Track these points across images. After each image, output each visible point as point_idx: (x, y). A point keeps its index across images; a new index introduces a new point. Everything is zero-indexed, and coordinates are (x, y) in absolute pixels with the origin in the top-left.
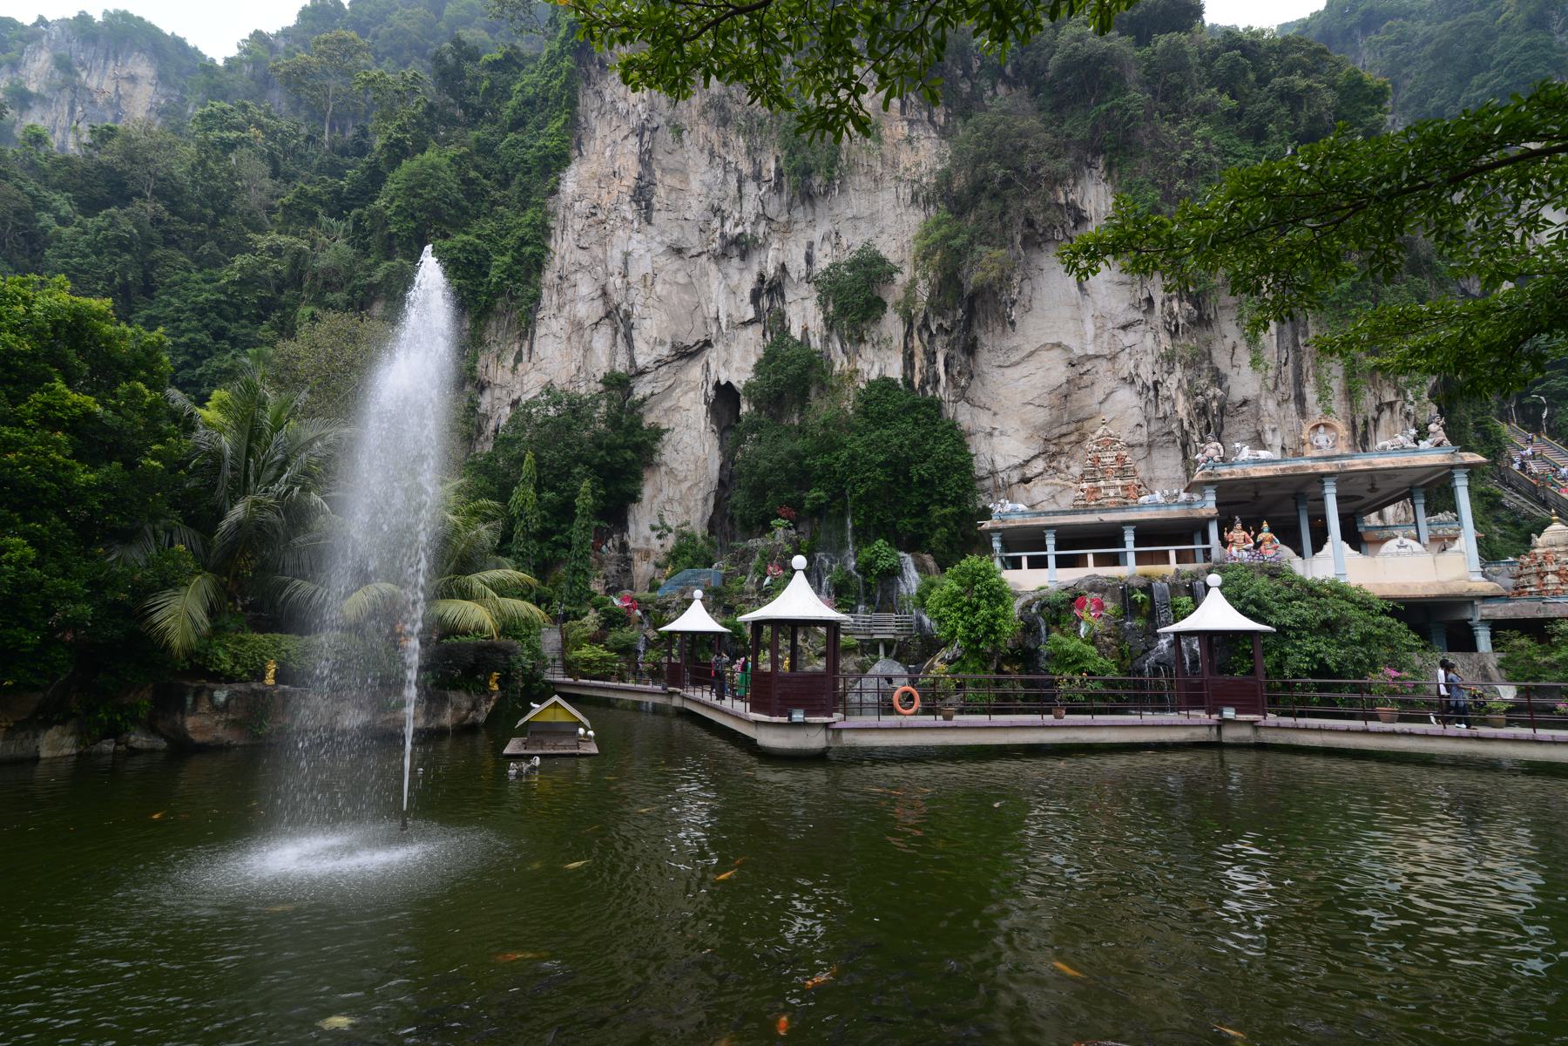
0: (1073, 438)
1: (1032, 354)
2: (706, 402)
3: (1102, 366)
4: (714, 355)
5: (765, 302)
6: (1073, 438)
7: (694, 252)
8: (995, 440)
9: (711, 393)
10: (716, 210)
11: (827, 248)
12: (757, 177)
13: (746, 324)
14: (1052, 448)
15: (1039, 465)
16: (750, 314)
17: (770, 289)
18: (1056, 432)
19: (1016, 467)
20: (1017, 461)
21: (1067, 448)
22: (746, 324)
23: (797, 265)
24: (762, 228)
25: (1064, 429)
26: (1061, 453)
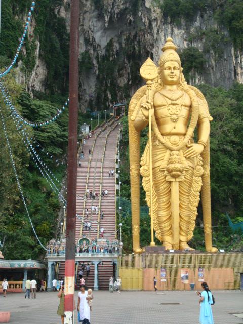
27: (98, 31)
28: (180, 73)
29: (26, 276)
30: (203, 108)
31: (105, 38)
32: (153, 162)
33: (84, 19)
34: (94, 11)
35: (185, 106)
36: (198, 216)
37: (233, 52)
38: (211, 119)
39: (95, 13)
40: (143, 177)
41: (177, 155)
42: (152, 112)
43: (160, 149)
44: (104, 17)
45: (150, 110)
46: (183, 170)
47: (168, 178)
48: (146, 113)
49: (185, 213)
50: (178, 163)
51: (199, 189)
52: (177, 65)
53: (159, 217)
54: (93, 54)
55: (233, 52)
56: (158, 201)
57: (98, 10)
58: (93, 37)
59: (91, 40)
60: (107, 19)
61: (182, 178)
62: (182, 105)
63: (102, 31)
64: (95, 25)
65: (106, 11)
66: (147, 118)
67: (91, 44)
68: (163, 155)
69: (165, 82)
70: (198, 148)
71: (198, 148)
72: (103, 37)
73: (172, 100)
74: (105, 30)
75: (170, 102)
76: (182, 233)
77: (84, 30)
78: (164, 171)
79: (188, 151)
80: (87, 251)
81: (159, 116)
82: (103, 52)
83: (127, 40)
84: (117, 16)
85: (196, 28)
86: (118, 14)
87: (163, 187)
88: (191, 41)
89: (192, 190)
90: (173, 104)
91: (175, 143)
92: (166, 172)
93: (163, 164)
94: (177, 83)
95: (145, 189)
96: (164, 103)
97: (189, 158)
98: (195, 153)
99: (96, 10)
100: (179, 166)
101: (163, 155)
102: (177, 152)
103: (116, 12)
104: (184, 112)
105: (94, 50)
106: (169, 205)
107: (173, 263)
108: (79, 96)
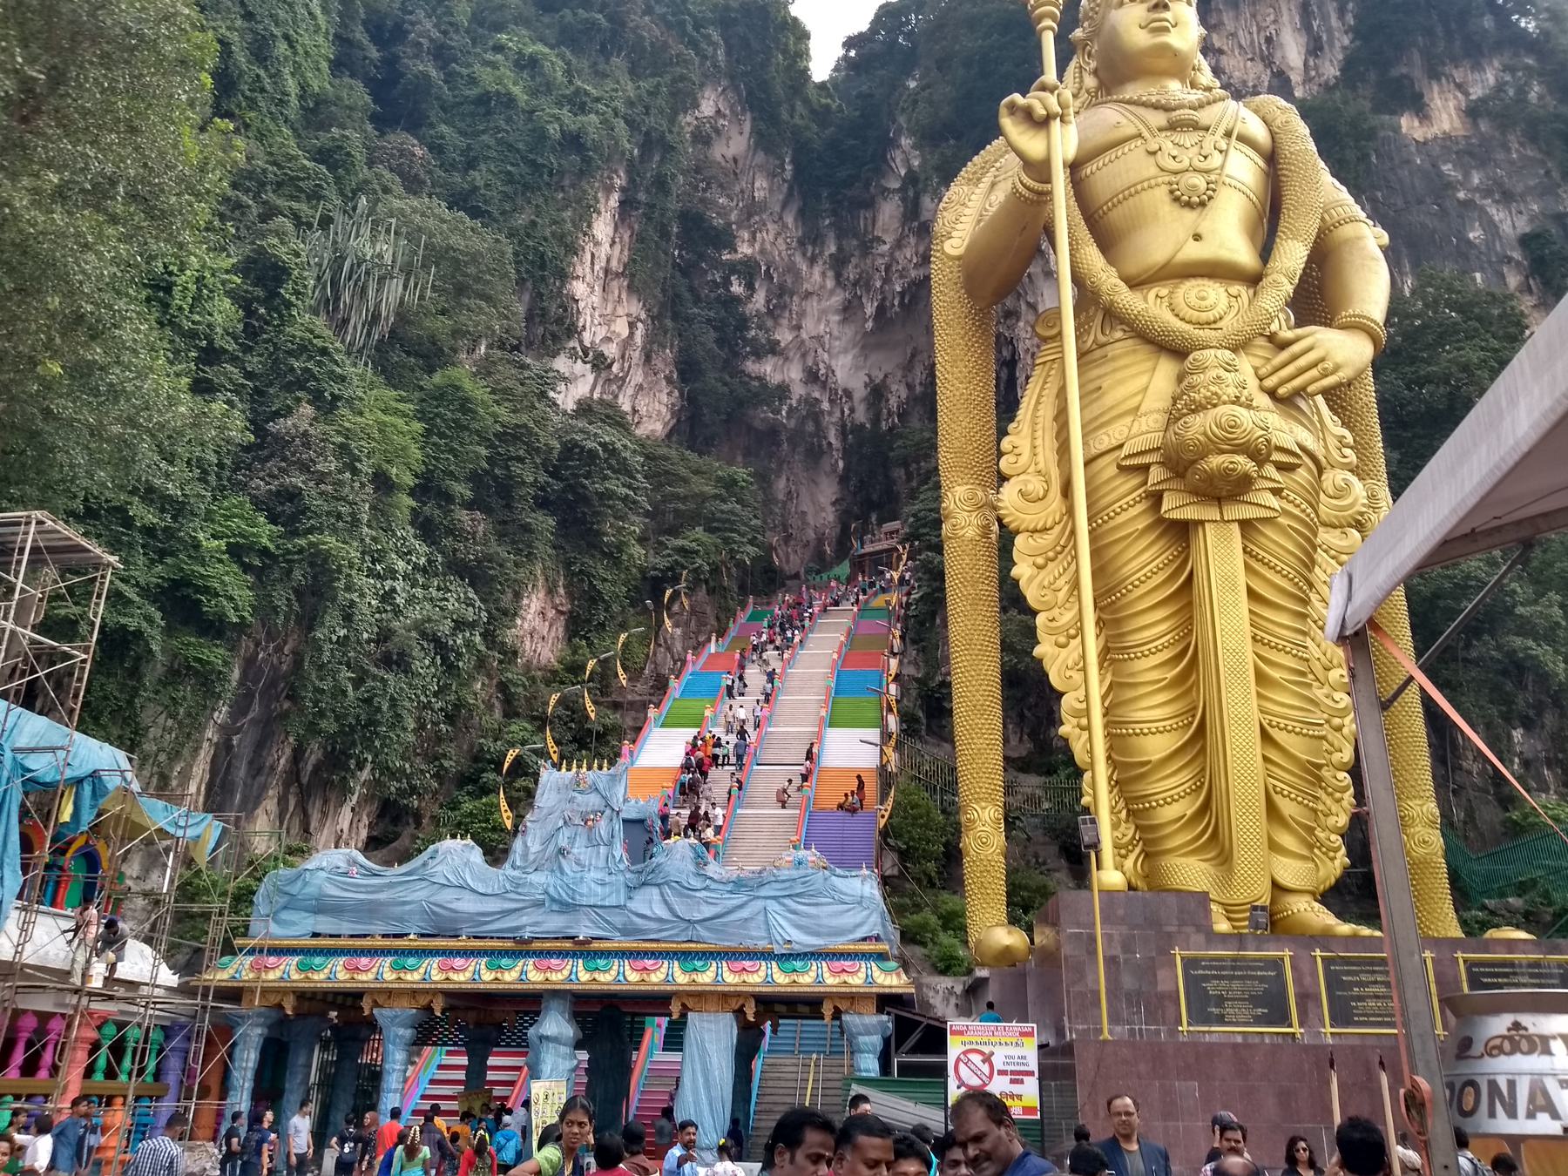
27: (845, 351)
33: (802, 314)
34: (832, 292)
35: (1242, 139)
39: (838, 299)
40: (1018, 532)
41: (1229, 367)
43: (1114, 359)
44: (862, 306)
45: (1056, 125)
46: (1267, 460)
47: (1175, 507)
48: (1033, 145)
50: (1236, 401)
54: (830, 413)
57: (844, 288)
58: (828, 367)
59: (823, 371)
60: (870, 309)
62: (1228, 134)
63: (855, 351)
64: (836, 333)
65: (868, 287)
67: (824, 385)
68: (1144, 379)
72: (857, 368)
73: (1167, 109)
74: (868, 344)
75: (1159, 119)
76: (1287, 840)
77: (803, 342)
78: (1145, 468)
79: (1284, 355)
82: (861, 416)
84: (902, 304)
86: (902, 294)
89: (1314, 597)
90: (1173, 127)
91: (1204, 316)
92: (1156, 474)
93: (1142, 431)
95: (1032, 595)
96: (1131, 130)
97: (1300, 392)
98: (1329, 365)
99: (839, 291)
101: (1144, 379)
103: (899, 289)
104: (1244, 169)
105: (831, 401)
106: (1190, 664)
107: (1284, 1019)
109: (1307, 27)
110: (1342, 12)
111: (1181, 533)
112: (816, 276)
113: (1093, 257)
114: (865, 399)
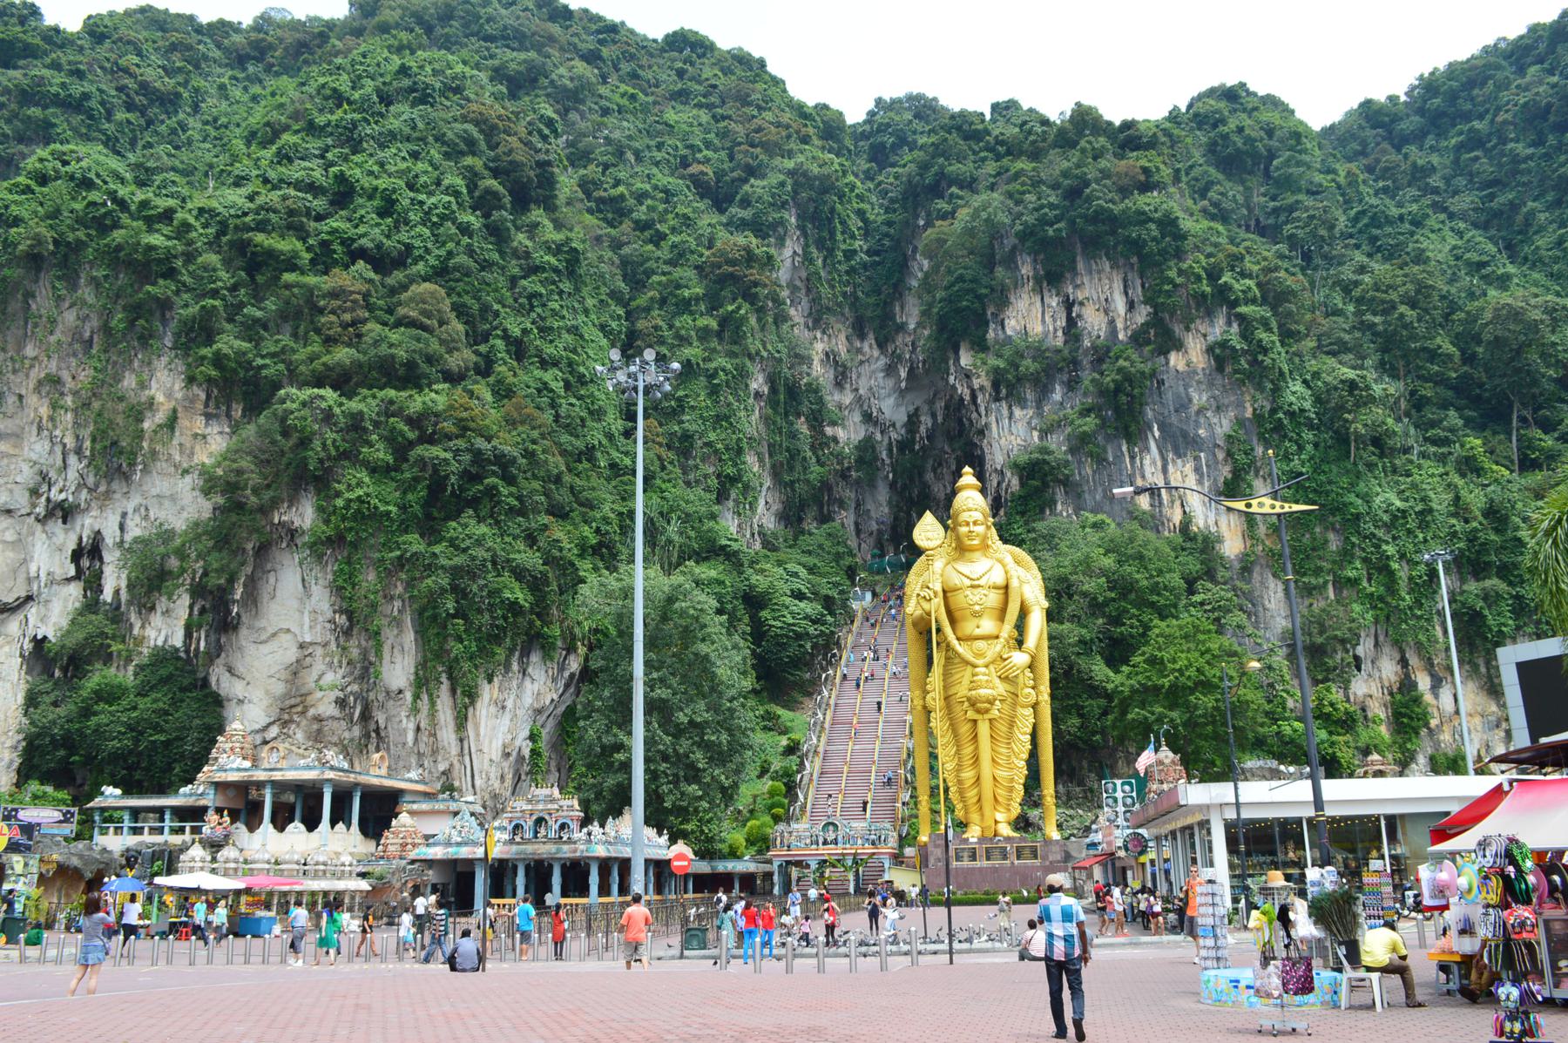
0: (299, 709)
1: (274, 635)
2: (22, 655)
3: (319, 651)
4: (34, 610)
5: (85, 563)
6: (299, 709)
7: (24, 512)
8: (245, 707)
9: (28, 646)
10: (44, 477)
11: (137, 519)
12: (78, 451)
13: (69, 580)
14: (286, 717)
15: (274, 731)
16: (72, 572)
17: (88, 555)
18: (288, 703)
19: (257, 732)
20: (257, 727)
21: (295, 717)
22: (69, 580)
23: (111, 534)
24: (84, 494)
25: (293, 701)
26: (291, 721)
28: (988, 528)
29: (737, 886)
30: (1032, 588)
31: (903, 409)
32: (946, 688)
36: (1027, 777)
37: (1124, 448)
38: (1046, 604)
39: (883, 361)
42: (939, 601)
47: (971, 714)
49: (1002, 774)
51: (1029, 730)
52: (978, 516)
53: (960, 782)
55: (1124, 448)
56: (958, 752)
60: (903, 374)
61: (995, 713)
65: (900, 358)
66: (929, 614)
67: (876, 423)
69: (961, 550)
70: (1020, 659)
71: (1020, 659)
72: (898, 406)
74: (903, 393)
75: (968, 583)
80: (835, 842)
81: (953, 607)
83: (947, 407)
85: (1055, 403)
86: (924, 362)
87: (965, 729)
88: (1044, 433)
90: (973, 587)
94: (985, 547)
100: (983, 692)
102: (983, 670)
104: (994, 598)
108: (857, 524)
109: (1126, 293)
110: (1143, 286)
111: (975, 721)
112: (869, 347)
113: (948, 630)
114: (905, 425)
